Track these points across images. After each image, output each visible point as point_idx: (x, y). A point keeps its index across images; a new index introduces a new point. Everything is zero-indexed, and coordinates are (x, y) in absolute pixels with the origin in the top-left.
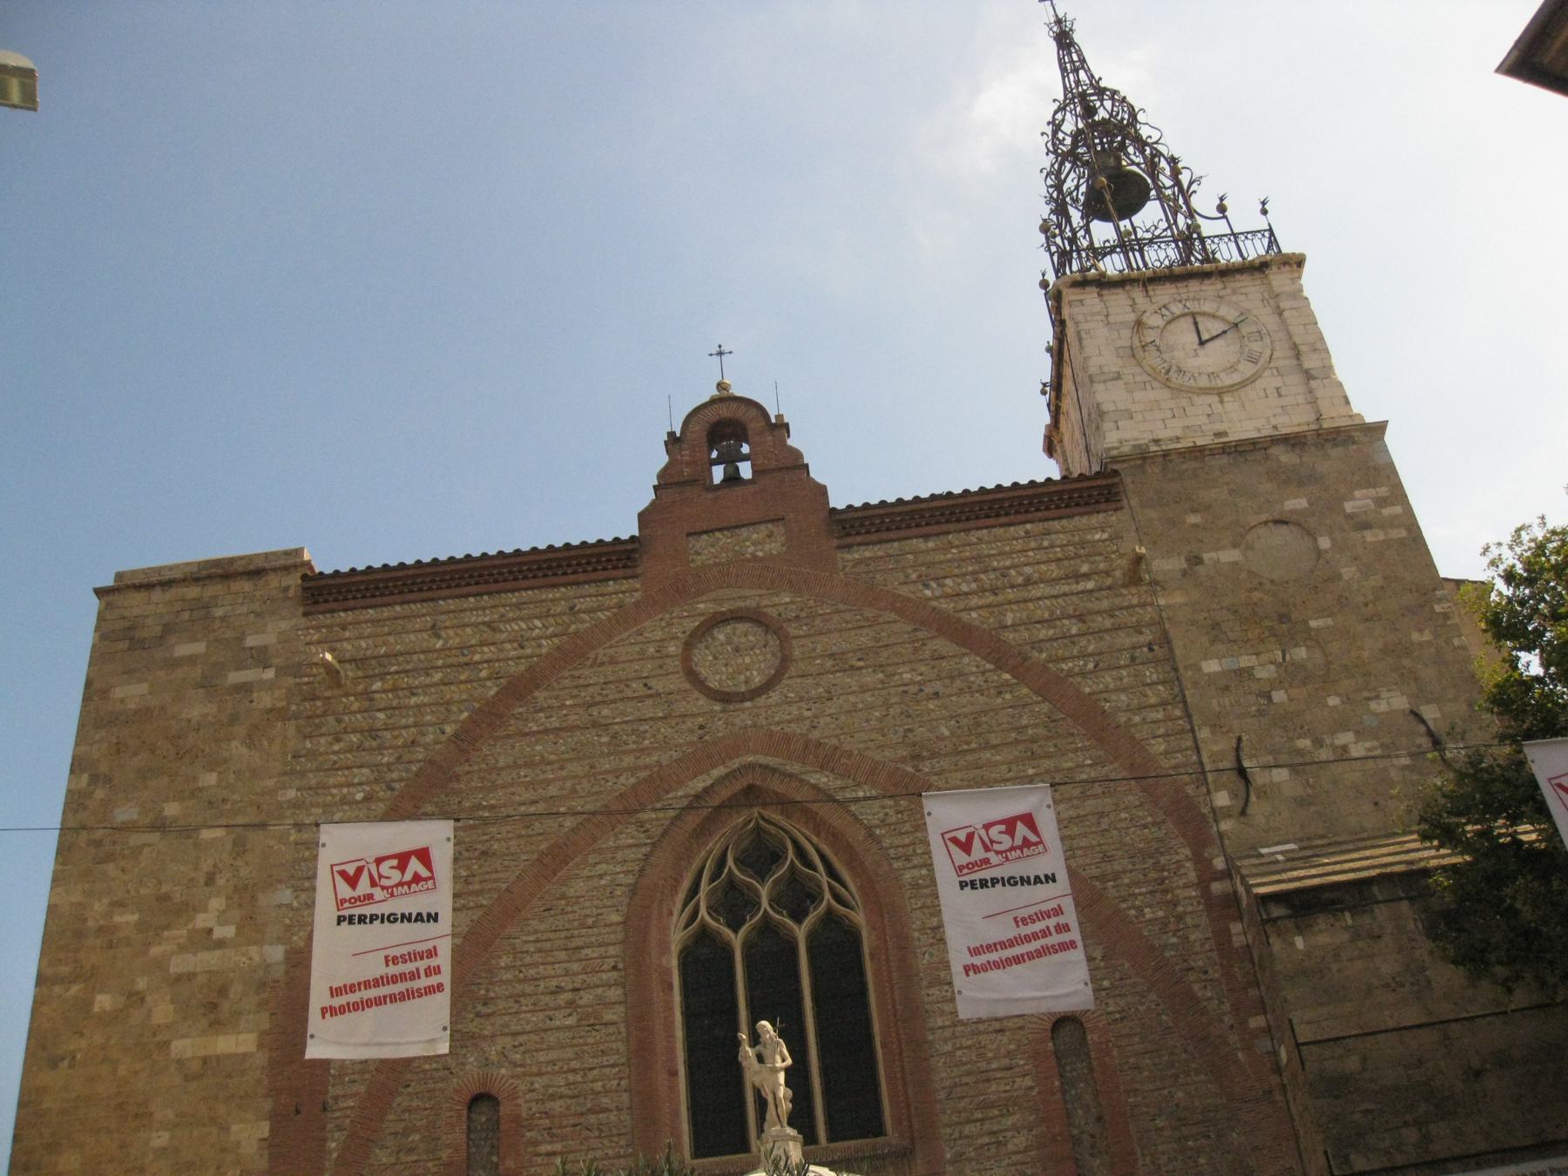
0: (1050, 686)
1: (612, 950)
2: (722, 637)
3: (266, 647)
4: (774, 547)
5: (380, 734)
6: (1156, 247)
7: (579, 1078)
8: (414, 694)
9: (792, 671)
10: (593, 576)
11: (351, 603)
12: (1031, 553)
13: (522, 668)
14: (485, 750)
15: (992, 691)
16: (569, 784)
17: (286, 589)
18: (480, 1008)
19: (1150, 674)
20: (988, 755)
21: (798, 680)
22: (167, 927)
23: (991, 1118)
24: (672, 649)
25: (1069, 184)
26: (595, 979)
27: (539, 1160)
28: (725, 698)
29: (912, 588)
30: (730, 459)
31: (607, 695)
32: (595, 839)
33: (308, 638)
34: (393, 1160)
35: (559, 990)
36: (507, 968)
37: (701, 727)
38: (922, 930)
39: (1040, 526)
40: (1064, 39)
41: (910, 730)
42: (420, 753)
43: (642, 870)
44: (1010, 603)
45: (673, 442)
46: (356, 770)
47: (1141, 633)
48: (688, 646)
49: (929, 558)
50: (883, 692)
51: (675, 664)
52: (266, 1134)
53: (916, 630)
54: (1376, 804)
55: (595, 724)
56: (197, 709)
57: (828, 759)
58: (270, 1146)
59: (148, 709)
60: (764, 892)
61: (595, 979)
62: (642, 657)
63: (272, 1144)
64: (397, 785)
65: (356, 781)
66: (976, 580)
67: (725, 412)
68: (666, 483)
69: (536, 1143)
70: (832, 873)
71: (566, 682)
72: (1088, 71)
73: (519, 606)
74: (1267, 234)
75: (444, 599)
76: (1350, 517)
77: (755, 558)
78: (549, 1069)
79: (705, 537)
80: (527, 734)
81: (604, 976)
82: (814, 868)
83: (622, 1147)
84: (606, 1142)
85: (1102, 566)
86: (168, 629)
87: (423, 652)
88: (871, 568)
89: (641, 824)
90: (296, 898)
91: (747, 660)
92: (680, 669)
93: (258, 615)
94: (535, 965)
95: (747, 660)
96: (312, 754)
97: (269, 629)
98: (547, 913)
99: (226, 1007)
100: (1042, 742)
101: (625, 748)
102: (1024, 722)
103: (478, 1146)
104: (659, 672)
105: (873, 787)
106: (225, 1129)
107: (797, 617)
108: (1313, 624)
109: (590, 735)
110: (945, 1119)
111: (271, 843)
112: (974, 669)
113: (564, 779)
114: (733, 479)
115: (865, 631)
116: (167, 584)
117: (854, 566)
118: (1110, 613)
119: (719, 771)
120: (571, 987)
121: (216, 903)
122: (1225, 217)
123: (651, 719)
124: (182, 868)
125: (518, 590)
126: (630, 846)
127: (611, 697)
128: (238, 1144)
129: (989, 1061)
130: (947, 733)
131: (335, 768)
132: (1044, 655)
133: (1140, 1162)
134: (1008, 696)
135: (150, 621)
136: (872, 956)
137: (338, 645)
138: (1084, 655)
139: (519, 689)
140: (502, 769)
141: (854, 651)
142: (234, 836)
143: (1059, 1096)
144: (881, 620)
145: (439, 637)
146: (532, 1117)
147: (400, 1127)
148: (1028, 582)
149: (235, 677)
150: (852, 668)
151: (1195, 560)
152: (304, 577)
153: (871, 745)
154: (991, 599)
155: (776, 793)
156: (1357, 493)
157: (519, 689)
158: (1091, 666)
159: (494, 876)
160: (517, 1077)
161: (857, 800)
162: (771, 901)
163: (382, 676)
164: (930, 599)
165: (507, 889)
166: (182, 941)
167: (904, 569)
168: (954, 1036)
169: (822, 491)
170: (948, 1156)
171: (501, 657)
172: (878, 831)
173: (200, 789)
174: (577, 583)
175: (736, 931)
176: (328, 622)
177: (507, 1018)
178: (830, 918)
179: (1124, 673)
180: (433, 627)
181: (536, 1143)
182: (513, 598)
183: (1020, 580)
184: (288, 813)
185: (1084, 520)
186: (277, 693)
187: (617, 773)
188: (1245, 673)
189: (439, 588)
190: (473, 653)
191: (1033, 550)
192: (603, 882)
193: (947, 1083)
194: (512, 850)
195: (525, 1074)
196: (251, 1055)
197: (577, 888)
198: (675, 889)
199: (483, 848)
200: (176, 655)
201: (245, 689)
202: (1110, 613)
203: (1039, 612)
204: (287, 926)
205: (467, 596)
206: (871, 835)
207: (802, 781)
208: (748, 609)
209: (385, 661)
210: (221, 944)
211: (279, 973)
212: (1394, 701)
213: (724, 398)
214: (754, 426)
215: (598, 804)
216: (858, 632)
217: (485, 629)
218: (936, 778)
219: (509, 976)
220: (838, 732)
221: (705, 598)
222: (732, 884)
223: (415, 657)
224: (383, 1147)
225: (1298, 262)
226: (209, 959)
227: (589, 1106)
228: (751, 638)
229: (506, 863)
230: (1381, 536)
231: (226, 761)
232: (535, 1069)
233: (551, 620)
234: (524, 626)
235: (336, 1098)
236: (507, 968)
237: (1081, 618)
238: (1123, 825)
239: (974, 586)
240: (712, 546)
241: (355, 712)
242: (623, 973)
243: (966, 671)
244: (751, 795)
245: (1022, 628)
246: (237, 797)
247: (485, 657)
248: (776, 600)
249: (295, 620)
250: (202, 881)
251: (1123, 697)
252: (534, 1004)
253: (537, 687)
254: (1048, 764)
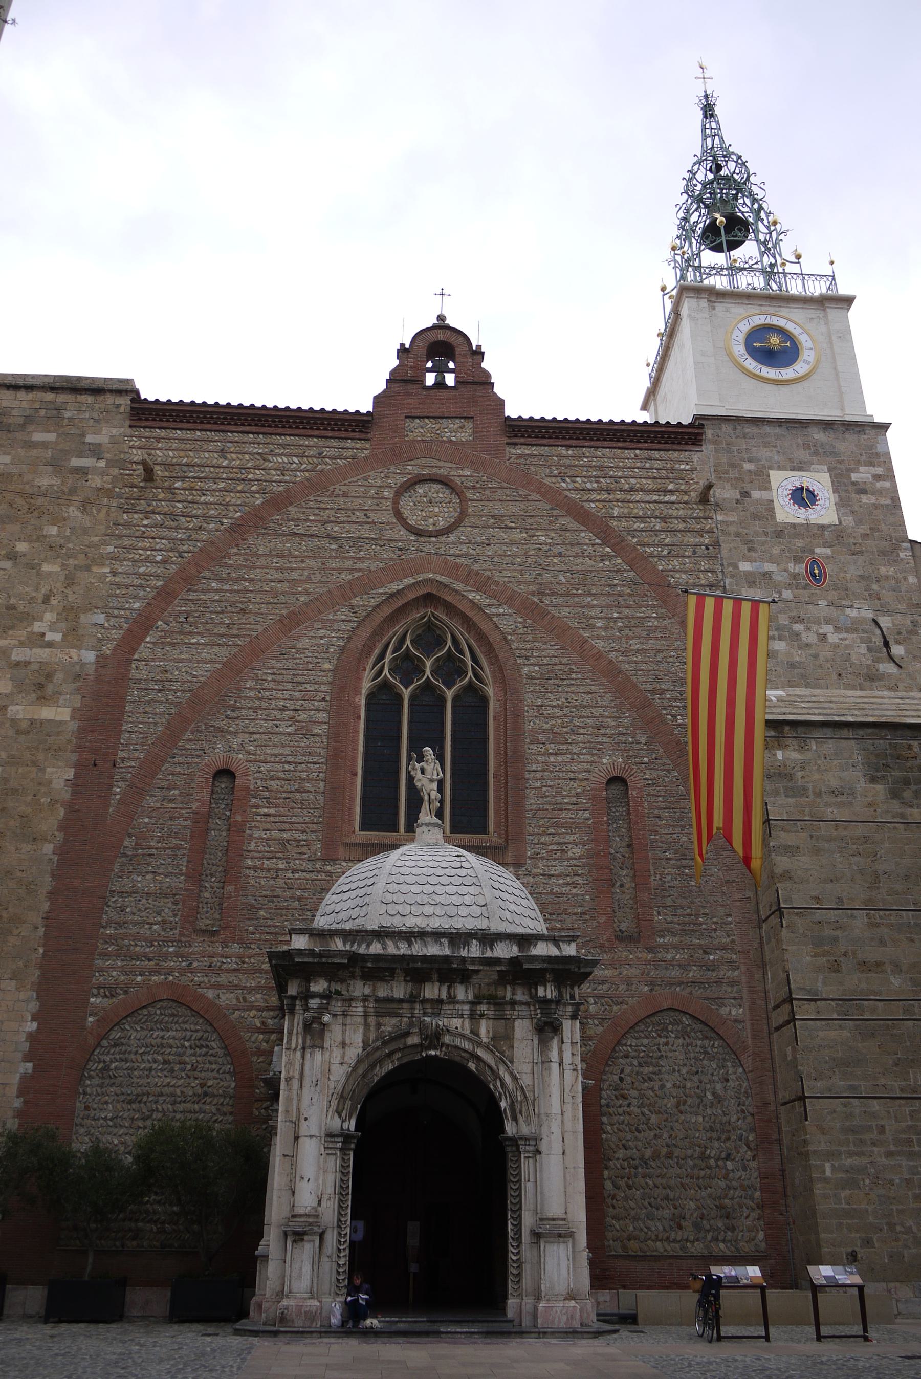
0: (636, 561)
1: (323, 688)
2: (421, 491)
3: (100, 445)
4: (465, 436)
5: (177, 518)
6: (752, 274)
7: (292, 768)
8: (204, 495)
9: (466, 522)
10: (337, 434)
11: (165, 424)
12: (636, 470)
13: (281, 489)
14: (250, 541)
15: (598, 558)
16: (306, 573)
17: (118, 406)
18: (229, 712)
19: (704, 565)
20: (589, 599)
21: (469, 529)
22: (12, 627)
23: (559, 834)
25: (694, 218)
26: (306, 704)
27: (259, 818)
28: (419, 533)
29: (554, 480)
30: (440, 370)
31: (338, 518)
32: (320, 612)
33: (132, 443)
34: (158, 805)
35: (284, 709)
36: (250, 689)
37: (401, 550)
38: (531, 706)
39: (645, 454)
40: (708, 111)
41: (539, 574)
42: (204, 536)
43: (349, 638)
44: (618, 501)
45: (403, 351)
46: (158, 540)
47: (702, 536)
49: (568, 462)
50: (525, 547)
52: (72, 777)
53: (552, 509)
54: (840, 675)
55: (329, 537)
56: (46, 480)
57: (483, 585)
58: (73, 784)
59: (9, 474)
60: (428, 664)
61: (306, 704)
62: (365, 496)
63: (75, 785)
64: (186, 555)
65: (157, 547)
66: (597, 482)
67: (441, 336)
68: (395, 378)
69: (258, 807)
70: (475, 659)
71: (311, 504)
72: (721, 139)
73: (283, 446)
74: (830, 279)
75: (232, 432)
76: (854, 484)
77: (450, 442)
78: (272, 759)
79: (417, 420)
80: (281, 535)
81: (316, 703)
82: (462, 653)
83: (315, 817)
84: (305, 812)
85: (683, 487)
86: (29, 420)
87: (214, 467)
88: (528, 462)
89: (352, 607)
90: (108, 621)
91: (437, 509)
92: (390, 508)
93: (97, 421)
94: (271, 689)
95: (437, 509)
96: (127, 525)
97: (104, 432)
98: (282, 657)
99: (50, 688)
100: (626, 597)
101: (347, 555)
102: (616, 582)
103: (217, 804)
104: (376, 508)
105: (510, 607)
106: (42, 770)
107: (474, 487)
108: (817, 550)
109: (325, 543)
110: (530, 829)
111: (93, 581)
112: (588, 541)
113: (304, 569)
114: (440, 384)
115: (517, 504)
116: (29, 388)
117: (516, 459)
118: (684, 519)
119: (409, 581)
120: (292, 708)
121: (49, 617)
122: (799, 263)
123: (367, 538)
124: (27, 589)
125: (285, 435)
126: (343, 621)
127: (342, 519)
128: (50, 782)
129: (563, 797)
130: (564, 580)
131: (143, 537)
132: (635, 540)
133: (653, 878)
134: (607, 563)
135: (14, 412)
136: (494, 717)
137: (153, 452)
138: (662, 545)
139: (278, 503)
140: (261, 555)
141: (509, 516)
142: (67, 572)
143: (605, 827)
144: (530, 498)
145: (226, 458)
146: (257, 789)
147: (165, 784)
148: (632, 490)
149: (75, 462)
150: (507, 527)
151: (746, 494)
152: (132, 400)
153: (513, 580)
154: (605, 496)
155: (446, 601)
156: (862, 469)
157: (278, 503)
158: (665, 552)
159: (248, 626)
160: (251, 762)
161: (498, 615)
162: (432, 672)
163: (183, 479)
164: (565, 490)
165: (256, 637)
166: (22, 638)
167: (549, 467)
168: (542, 778)
169: (500, 403)
170: (529, 853)
171: (267, 479)
172: (509, 637)
173: (45, 536)
174: (326, 437)
175: (406, 688)
176: (147, 434)
177: (247, 722)
178: (470, 688)
179: (687, 560)
180: (222, 451)
181: (258, 807)
182: (281, 440)
183: (627, 486)
184: (108, 562)
185: (676, 454)
186: (106, 478)
187: (340, 571)
188: (767, 575)
189: (229, 424)
190: (248, 473)
191: (638, 468)
192: (322, 641)
193: (534, 807)
194: (262, 610)
195: (255, 761)
196: (66, 722)
197: (305, 643)
198: (369, 653)
199: (243, 607)
200: (33, 439)
201: (83, 472)
202: (684, 519)
203: (636, 511)
204: (99, 638)
205: (248, 433)
206: (505, 639)
207: (463, 595)
208: (441, 476)
209: (185, 468)
210: (50, 644)
211: (91, 670)
212: (862, 612)
213: (441, 325)
214: (460, 350)
215: (325, 589)
216: (514, 503)
217: (258, 457)
218: (553, 608)
219: (252, 694)
220: (492, 567)
221: (413, 463)
222: (408, 656)
223: (207, 469)
224: (152, 796)
225: (848, 301)
226: (42, 654)
227: (296, 787)
228: (441, 495)
229: (258, 619)
230: (873, 500)
231: (64, 520)
232: (262, 758)
233: (305, 459)
234: (286, 460)
235: (123, 759)
236: (250, 689)
237: (664, 519)
238: (671, 660)
239: (595, 485)
240: (422, 428)
241: (160, 500)
242: (329, 703)
243: (582, 541)
244: (429, 599)
245: (623, 520)
246: (70, 546)
247: (257, 477)
248: (460, 472)
249: (122, 430)
250: (40, 601)
251: (684, 576)
252: (267, 716)
253: (291, 504)
254: (627, 611)
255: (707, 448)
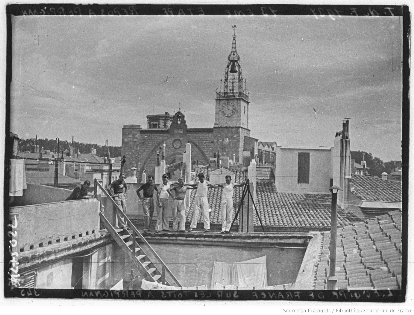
24: (172, 142)
40: (234, 39)
48: (173, 142)
51: (172, 144)
151: (218, 141)
169: (186, 126)
182: (159, 134)
213: (179, 113)
255: (214, 132)
